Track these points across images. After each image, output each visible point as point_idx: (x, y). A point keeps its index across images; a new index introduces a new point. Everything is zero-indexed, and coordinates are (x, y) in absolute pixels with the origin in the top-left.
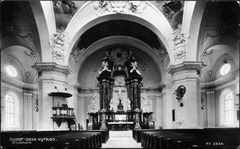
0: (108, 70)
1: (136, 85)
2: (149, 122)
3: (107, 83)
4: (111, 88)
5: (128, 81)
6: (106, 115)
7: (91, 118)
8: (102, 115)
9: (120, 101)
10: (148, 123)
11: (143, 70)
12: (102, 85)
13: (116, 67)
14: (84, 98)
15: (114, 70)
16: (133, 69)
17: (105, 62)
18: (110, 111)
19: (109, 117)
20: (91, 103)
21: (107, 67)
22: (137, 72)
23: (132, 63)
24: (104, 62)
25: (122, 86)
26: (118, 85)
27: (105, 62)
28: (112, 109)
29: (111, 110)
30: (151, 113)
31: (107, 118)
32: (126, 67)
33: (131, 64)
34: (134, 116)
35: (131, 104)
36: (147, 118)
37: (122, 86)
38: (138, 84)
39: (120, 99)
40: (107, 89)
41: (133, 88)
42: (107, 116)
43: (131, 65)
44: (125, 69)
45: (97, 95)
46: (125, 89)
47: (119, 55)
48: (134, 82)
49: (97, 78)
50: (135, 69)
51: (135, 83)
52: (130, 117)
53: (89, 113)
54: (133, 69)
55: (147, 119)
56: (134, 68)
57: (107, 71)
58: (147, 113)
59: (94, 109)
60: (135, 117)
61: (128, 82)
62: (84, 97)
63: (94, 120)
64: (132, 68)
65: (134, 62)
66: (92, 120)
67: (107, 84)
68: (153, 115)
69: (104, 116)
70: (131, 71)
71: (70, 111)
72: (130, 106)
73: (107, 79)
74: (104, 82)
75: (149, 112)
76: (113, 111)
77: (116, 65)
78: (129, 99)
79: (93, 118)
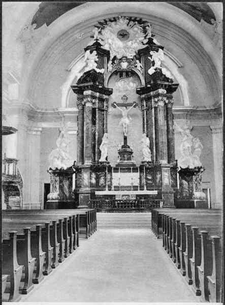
0: (98, 71)
1: (161, 104)
2: (193, 191)
3: (93, 97)
4: (103, 111)
5: (143, 94)
6: (91, 174)
7: (56, 181)
8: (81, 172)
9: (125, 138)
10: (191, 194)
11: (179, 67)
12: (83, 103)
13: (115, 62)
14: (41, 132)
15: (110, 68)
16: (155, 67)
17: (91, 52)
18: (101, 163)
19: (98, 178)
20: (58, 145)
21: (96, 62)
22: (164, 74)
23: (151, 53)
24: (88, 52)
25: (130, 105)
26: (121, 102)
27: (91, 52)
28: (106, 159)
29: (105, 160)
30: (198, 170)
31: (94, 181)
32: (140, 62)
33: (151, 56)
34: (158, 176)
35: (151, 148)
36: (188, 182)
37: (130, 105)
38: (167, 99)
39: (125, 135)
40: (94, 111)
41: (156, 108)
42: (94, 175)
43: (149, 58)
44: (136, 67)
45: (71, 129)
46: (138, 111)
47: (123, 35)
48: (158, 95)
49: (72, 87)
50: (159, 67)
51: (160, 98)
52: (150, 178)
53: (51, 169)
54: (153, 65)
55: (189, 184)
56: (157, 65)
57: (95, 72)
58: (188, 169)
59: (63, 159)
60: (161, 179)
61: (143, 96)
62: (40, 129)
63: (63, 185)
64: (153, 63)
65: (157, 51)
66: (58, 186)
67: (94, 101)
68: (203, 176)
69: (85, 176)
70: (151, 71)
71: (11, 165)
72: (149, 150)
73: (94, 88)
74: (87, 96)
75: (192, 167)
76: (108, 163)
77: (115, 58)
78: (145, 134)
79: (61, 181)
